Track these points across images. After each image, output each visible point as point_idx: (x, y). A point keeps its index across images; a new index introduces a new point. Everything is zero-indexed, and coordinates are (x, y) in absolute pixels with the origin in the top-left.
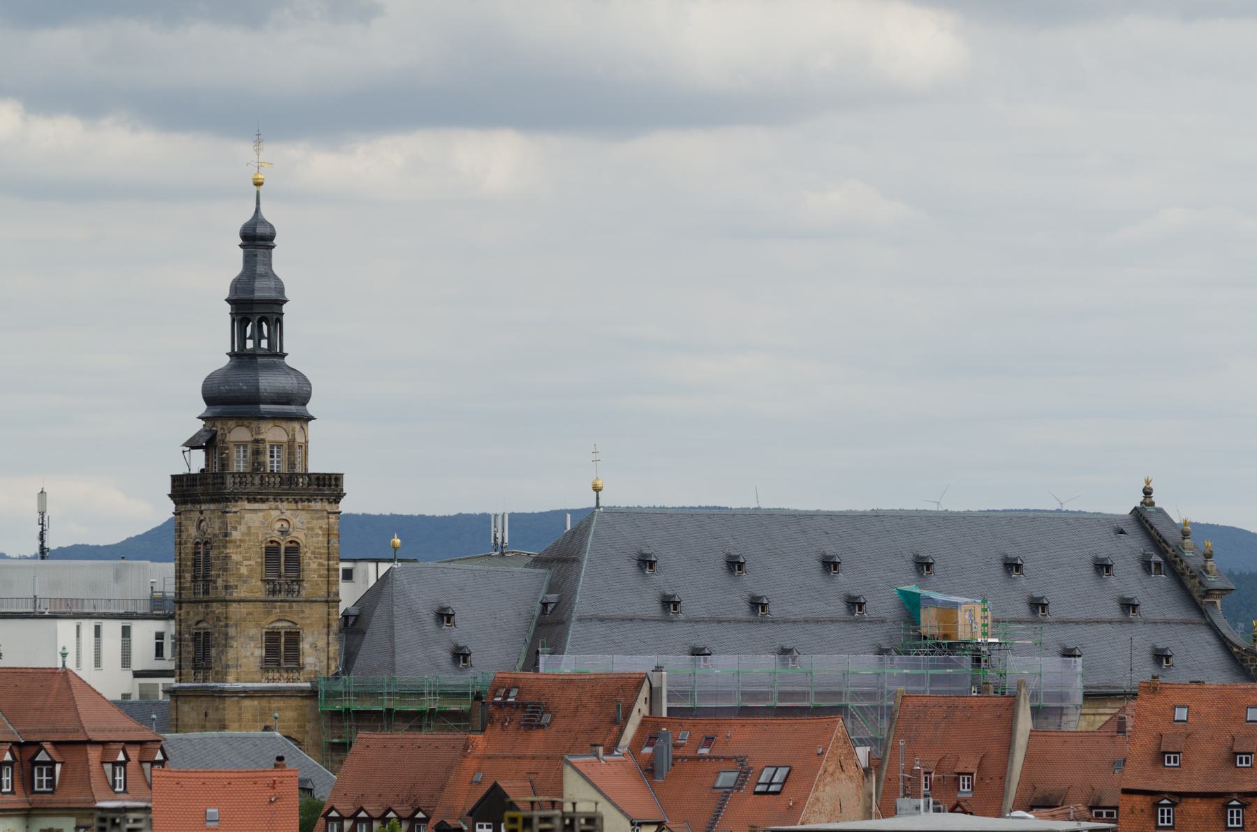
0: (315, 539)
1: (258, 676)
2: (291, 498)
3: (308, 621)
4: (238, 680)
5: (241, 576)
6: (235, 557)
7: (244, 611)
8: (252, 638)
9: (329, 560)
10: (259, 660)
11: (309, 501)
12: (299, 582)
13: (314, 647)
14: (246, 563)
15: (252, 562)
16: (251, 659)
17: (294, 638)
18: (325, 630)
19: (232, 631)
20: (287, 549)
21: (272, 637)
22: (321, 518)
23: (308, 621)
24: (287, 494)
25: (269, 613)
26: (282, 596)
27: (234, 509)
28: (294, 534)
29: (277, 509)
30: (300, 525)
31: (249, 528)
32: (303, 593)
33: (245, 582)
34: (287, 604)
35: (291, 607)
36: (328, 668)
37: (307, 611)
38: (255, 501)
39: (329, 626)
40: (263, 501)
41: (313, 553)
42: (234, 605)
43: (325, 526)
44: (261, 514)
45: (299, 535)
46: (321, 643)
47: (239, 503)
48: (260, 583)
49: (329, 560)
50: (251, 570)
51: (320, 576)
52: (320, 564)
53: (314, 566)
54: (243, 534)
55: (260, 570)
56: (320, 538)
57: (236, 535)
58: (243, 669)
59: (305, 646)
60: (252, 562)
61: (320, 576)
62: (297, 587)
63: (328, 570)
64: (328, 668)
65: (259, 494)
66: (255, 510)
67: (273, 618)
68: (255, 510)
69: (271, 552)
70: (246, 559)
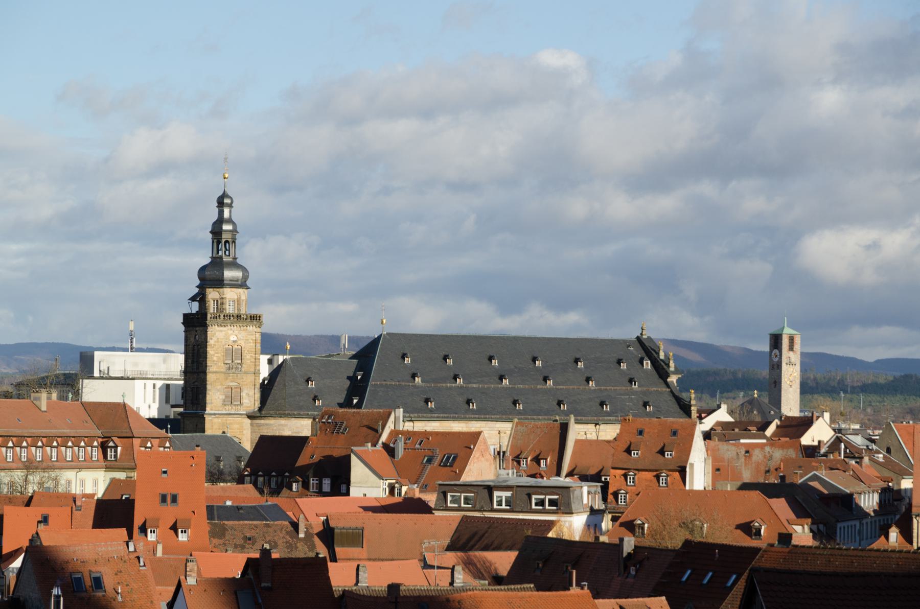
0: (249, 345)
3: (245, 383)
5: (214, 361)
7: (215, 377)
8: (218, 390)
15: (219, 355)
18: (254, 387)
22: (252, 335)
23: (245, 383)
25: (227, 379)
29: (231, 330)
30: (242, 338)
31: (218, 339)
32: (243, 370)
35: (237, 376)
37: (245, 378)
41: (248, 351)
44: (223, 333)
46: (252, 393)
51: (251, 362)
52: (251, 356)
53: (248, 357)
56: (252, 344)
59: (244, 394)
61: (251, 362)
63: (255, 359)
66: (221, 331)
68: (221, 331)
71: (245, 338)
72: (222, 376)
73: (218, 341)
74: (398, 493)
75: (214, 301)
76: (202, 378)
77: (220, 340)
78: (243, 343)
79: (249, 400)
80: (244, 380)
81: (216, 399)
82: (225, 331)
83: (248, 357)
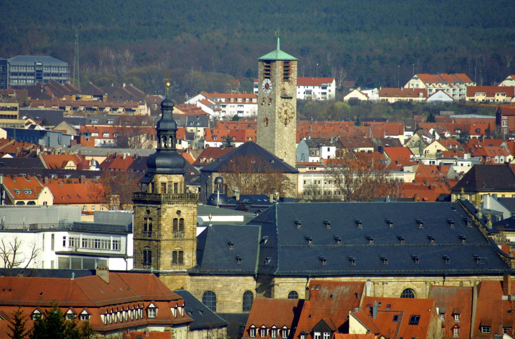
1: (170, 268)
3: (186, 247)
4: (163, 269)
5: (165, 231)
6: (164, 225)
7: (166, 244)
8: (168, 254)
10: (170, 262)
13: (188, 257)
14: (167, 227)
15: (169, 226)
16: (168, 261)
17: (181, 252)
18: (192, 250)
19: (162, 251)
21: (175, 253)
22: (191, 209)
23: (186, 247)
24: (181, 201)
25: (174, 244)
26: (178, 238)
27: (164, 207)
29: (177, 206)
30: (184, 212)
31: (168, 214)
34: (180, 241)
35: (181, 242)
36: (193, 264)
38: (170, 204)
39: (193, 249)
40: (173, 204)
41: (188, 222)
42: (163, 242)
45: (183, 216)
46: (190, 255)
47: (165, 204)
51: (190, 231)
52: (191, 227)
53: (189, 227)
55: (171, 229)
56: (191, 217)
57: (164, 216)
58: (165, 265)
59: (185, 256)
60: (169, 226)
61: (190, 231)
63: (193, 228)
64: (193, 264)
66: (170, 207)
67: (175, 246)
68: (170, 207)
70: (167, 225)
71: (186, 213)
72: (170, 243)
73: (168, 216)
77: (169, 215)
79: (189, 261)
80: (186, 245)
81: (166, 261)
83: (189, 227)
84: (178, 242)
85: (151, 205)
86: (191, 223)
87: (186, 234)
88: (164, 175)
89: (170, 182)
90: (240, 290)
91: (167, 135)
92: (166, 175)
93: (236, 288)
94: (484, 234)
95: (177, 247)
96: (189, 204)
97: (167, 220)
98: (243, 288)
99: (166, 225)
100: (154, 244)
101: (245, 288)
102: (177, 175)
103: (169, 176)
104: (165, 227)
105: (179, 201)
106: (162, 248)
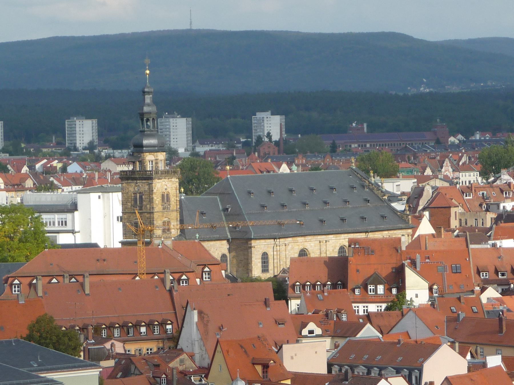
0: (173, 191)
2: (168, 178)
5: (156, 204)
6: (155, 198)
9: (176, 197)
11: (172, 178)
12: (169, 205)
14: (157, 200)
17: (169, 223)
20: (167, 194)
22: (174, 184)
24: (167, 177)
27: (155, 182)
28: (168, 189)
30: (169, 186)
31: (158, 188)
32: (171, 208)
33: (157, 206)
34: (167, 212)
35: (168, 213)
37: (172, 214)
38: (159, 179)
40: (161, 179)
43: (175, 186)
44: (160, 183)
45: (169, 190)
48: (161, 206)
49: (176, 197)
50: (159, 202)
52: (175, 199)
53: (173, 200)
54: (156, 190)
56: (174, 190)
61: (174, 203)
62: (169, 207)
63: (176, 201)
65: (161, 177)
68: (159, 182)
69: (163, 196)
70: (158, 198)
71: (171, 186)
72: (160, 214)
73: (157, 190)
74: (435, 292)
75: (149, 161)
76: (147, 216)
77: (159, 189)
78: (170, 190)
82: (161, 182)
83: (173, 200)
84: (166, 213)
85: (141, 181)
86: (174, 195)
87: (171, 206)
88: (150, 153)
89: (157, 160)
90: (218, 254)
91: (150, 117)
92: (153, 153)
93: (215, 252)
94: (380, 196)
95: (166, 218)
96: (172, 179)
97: (157, 194)
98: (220, 252)
99: (157, 199)
100: (146, 216)
101: (221, 252)
102: (162, 153)
103: (155, 154)
104: (156, 200)
105: (165, 177)
106: (154, 219)
